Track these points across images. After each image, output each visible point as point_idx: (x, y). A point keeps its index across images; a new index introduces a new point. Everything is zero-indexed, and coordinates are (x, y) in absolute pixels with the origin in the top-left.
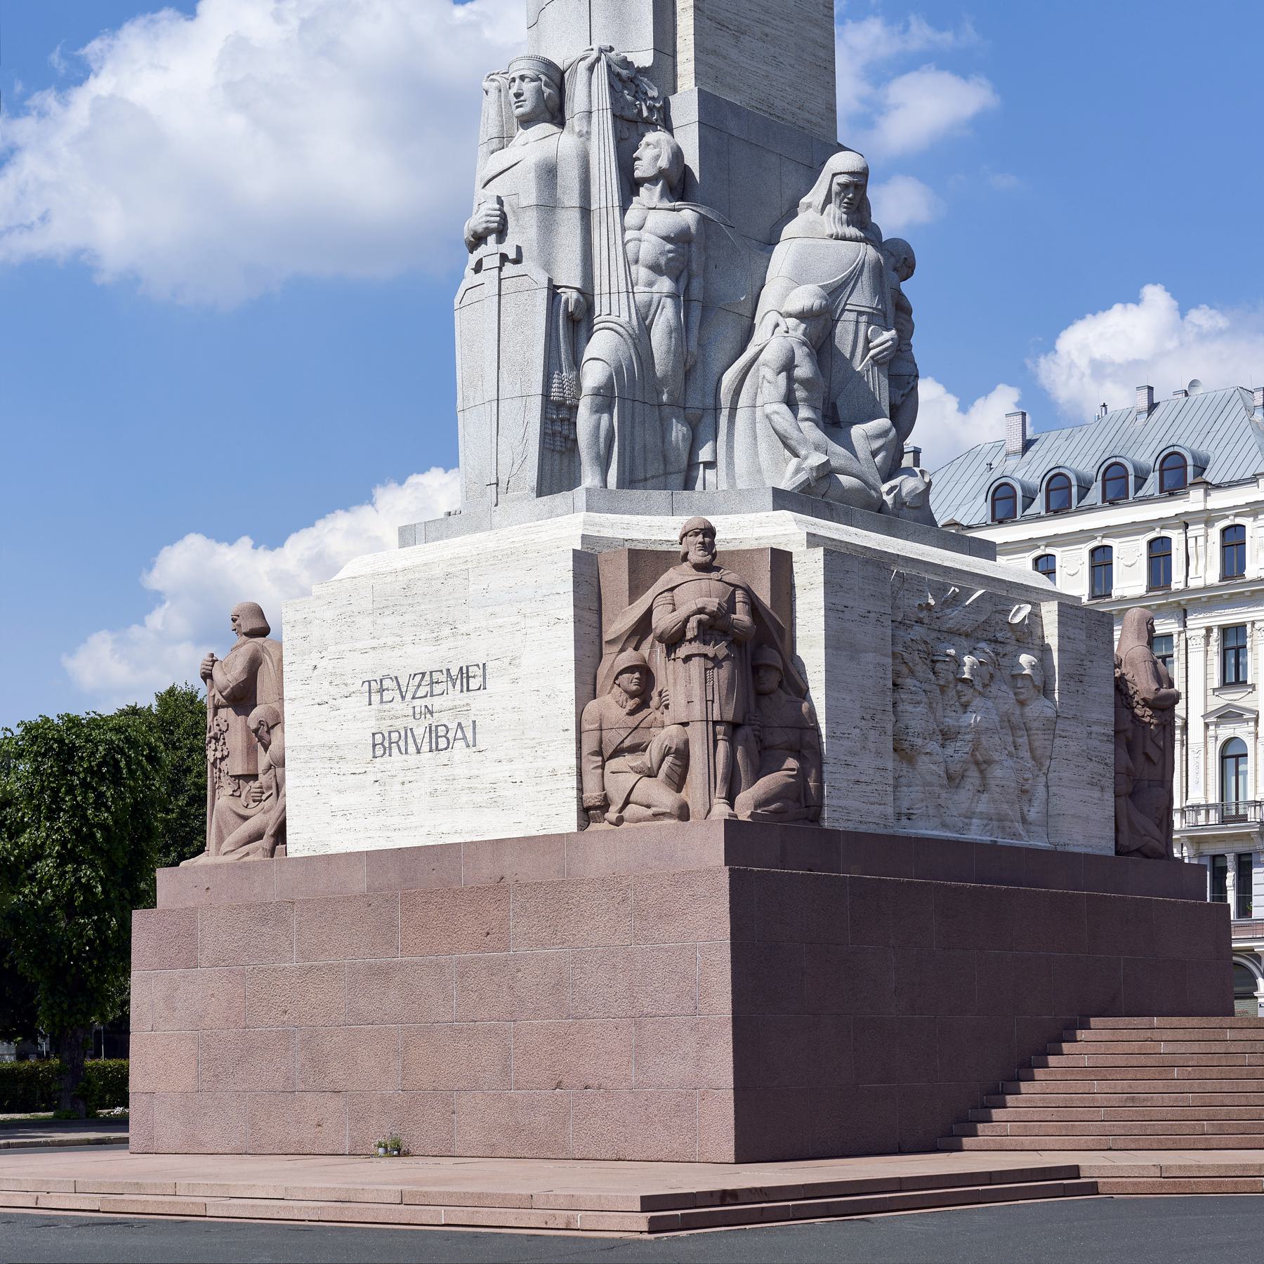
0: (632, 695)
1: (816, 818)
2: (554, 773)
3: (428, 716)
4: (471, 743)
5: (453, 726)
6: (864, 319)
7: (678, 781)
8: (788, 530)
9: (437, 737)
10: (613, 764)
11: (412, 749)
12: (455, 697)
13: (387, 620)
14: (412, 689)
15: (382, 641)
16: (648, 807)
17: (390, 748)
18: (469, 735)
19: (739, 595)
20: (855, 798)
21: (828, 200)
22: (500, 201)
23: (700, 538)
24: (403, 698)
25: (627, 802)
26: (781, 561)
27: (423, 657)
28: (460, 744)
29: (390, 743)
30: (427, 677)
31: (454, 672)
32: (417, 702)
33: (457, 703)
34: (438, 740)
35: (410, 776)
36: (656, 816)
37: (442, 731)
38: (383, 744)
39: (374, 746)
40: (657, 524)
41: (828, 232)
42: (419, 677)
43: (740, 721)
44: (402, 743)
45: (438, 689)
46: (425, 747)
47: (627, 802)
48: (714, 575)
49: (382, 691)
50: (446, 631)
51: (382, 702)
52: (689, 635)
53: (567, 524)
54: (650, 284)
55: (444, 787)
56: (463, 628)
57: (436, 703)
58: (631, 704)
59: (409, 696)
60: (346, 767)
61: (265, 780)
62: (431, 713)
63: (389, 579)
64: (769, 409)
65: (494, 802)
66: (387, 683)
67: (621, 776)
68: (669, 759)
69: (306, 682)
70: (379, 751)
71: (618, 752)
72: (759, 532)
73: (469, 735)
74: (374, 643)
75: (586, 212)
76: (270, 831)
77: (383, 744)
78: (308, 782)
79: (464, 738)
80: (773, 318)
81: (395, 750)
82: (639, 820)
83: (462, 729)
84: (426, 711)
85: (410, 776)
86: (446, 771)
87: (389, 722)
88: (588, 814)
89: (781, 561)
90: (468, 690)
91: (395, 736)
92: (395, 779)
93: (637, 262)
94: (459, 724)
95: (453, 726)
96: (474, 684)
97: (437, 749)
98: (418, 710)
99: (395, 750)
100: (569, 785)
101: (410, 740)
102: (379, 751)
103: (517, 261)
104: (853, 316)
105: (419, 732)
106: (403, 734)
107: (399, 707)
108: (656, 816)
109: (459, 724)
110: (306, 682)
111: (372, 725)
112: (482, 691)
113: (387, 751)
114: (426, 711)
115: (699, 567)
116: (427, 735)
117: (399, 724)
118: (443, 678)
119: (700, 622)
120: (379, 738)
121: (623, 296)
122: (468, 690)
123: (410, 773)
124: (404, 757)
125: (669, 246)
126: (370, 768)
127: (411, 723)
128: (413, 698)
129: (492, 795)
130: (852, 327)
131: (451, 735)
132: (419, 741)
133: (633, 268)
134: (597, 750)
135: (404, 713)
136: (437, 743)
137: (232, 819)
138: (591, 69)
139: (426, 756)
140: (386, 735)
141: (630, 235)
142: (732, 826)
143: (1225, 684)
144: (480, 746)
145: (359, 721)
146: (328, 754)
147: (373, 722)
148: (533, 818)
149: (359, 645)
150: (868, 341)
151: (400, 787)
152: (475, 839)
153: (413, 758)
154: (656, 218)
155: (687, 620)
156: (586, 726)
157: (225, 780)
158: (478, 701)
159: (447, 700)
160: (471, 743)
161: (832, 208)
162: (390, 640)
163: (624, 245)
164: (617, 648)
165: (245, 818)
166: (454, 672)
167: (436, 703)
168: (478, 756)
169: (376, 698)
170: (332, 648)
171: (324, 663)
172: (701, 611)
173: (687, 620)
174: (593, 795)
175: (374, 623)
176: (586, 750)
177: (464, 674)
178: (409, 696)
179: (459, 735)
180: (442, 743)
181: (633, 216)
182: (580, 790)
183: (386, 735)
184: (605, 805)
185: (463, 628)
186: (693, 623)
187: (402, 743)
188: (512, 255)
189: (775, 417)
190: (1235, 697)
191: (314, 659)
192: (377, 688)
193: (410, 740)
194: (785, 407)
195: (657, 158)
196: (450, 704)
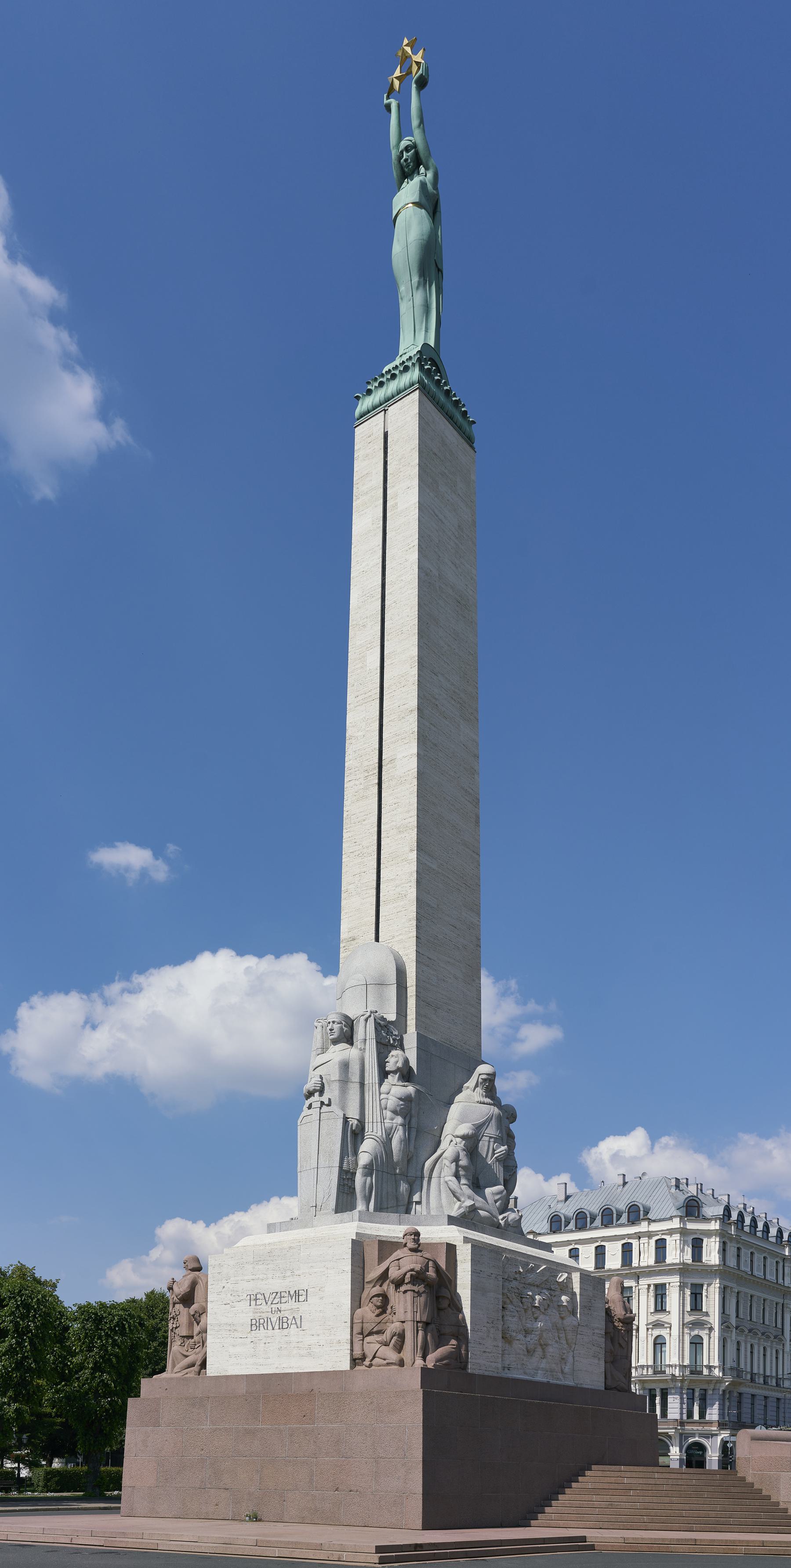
0: (378, 1307)
1: (465, 1368)
5: (290, 1317)
6: (492, 1140)
7: (399, 1348)
8: (454, 1234)
10: (368, 1339)
11: (270, 1327)
12: (292, 1304)
14: (271, 1299)
18: (299, 1323)
19: (431, 1264)
20: (483, 1360)
21: (476, 1086)
22: (321, 1077)
23: (413, 1237)
25: (374, 1357)
26: (451, 1249)
27: (277, 1284)
28: (294, 1326)
31: (292, 1293)
32: (273, 1306)
34: (283, 1324)
35: (269, 1340)
36: (388, 1364)
37: (285, 1320)
38: (256, 1325)
40: (393, 1229)
41: (476, 1100)
43: (429, 1321)
44: (265, 1325)
45: (283, 1300)
46: (277, 1327)
47: (374, 1357)
48: (419, 1254)
49: (256, 1299)
50: (289, 1273)
52: (406, 1281)
53: (349, 1227)
54: (392, 1119)
57: (283, 1307)
58: (378, 1311)
59: (269, 1303)
61: (197, 1338)
63: (262, 1248)
64: (447, 1179)
66: (259, 1296)
67: (372, 1345)
68: (395, 1338)
69: (219, 1294)
70: (254, 1328)
71: (370, 1334)
72: (441, 1235)
73: (299, 1323)
74: (253, 1277)
75: (362, 1084)
76: (198, 1363)
77: (256, 1325)
78: (218, 1341)
80: (450, 1137)
84: (276, 1311)
85: (269, 1340)
86: (286, 1339)
88: (355, 1361)
89: (451, 1249)
91: (262, 1321)
93: (386, 1109)
95: (290, 1317)
96: (301, 1298)
102: (254, 1328)
103: (329, 1105)
104: (487, 1139)
105: (274, 1320)
107: (264, 1307)
108: (388, 1364)
111: (251, 1315)
114: (276, 1311)
115: (411, 1250)
117: (264, 1315)
118: (286, 1295)
119: (411, 1275)
120: (254, 1322)
121: (379, 1124)
125: (401, 1103)
126: (249, 1335)
130: (487, 1144)
131: (289, 1322)
133: (384, 1111)
134: (360, 1332)
137: (180, 1356)
138: (366, 1020)
139: (277, 1331)
141: (383, 1096)
142: (425, 1370)
145: (244, 1313)
149: (246, 1278)
150: (494, 1150)
153: (270, 1332)
154: (396, 1090)
155: (405, 1274)
156: (355, 1321)
157: (177, 1338)
158: (303, 1307)
159: (288, 1306)
161: (478, 1089)
162: (261, 1277)
163: (380, 1101)
164: (371, 1285)
165: (186, 1356)
166: (292, 1293)
167: (283, 1307)
169: (253, 1303)
172: (412, 1270)
173: (405, 1274)
174: (358, 1353)
175: (254, 1268)
176: (355, 1332)
177: (297, 1294)
178: (269, 1303)
179: (294, 1322)
180: (285, 1325)
181: (384, 1088)
182: (352, 1350)
184: (364, 1358)
185: (297, 1273)
186: (408, 1275)
187: (265, 1325)
188: (326, 1102)
189: (450, 1183)
192: (254, 1298)
194: (454, 1179)
195: (397, 1062)
196: (290, 1308)
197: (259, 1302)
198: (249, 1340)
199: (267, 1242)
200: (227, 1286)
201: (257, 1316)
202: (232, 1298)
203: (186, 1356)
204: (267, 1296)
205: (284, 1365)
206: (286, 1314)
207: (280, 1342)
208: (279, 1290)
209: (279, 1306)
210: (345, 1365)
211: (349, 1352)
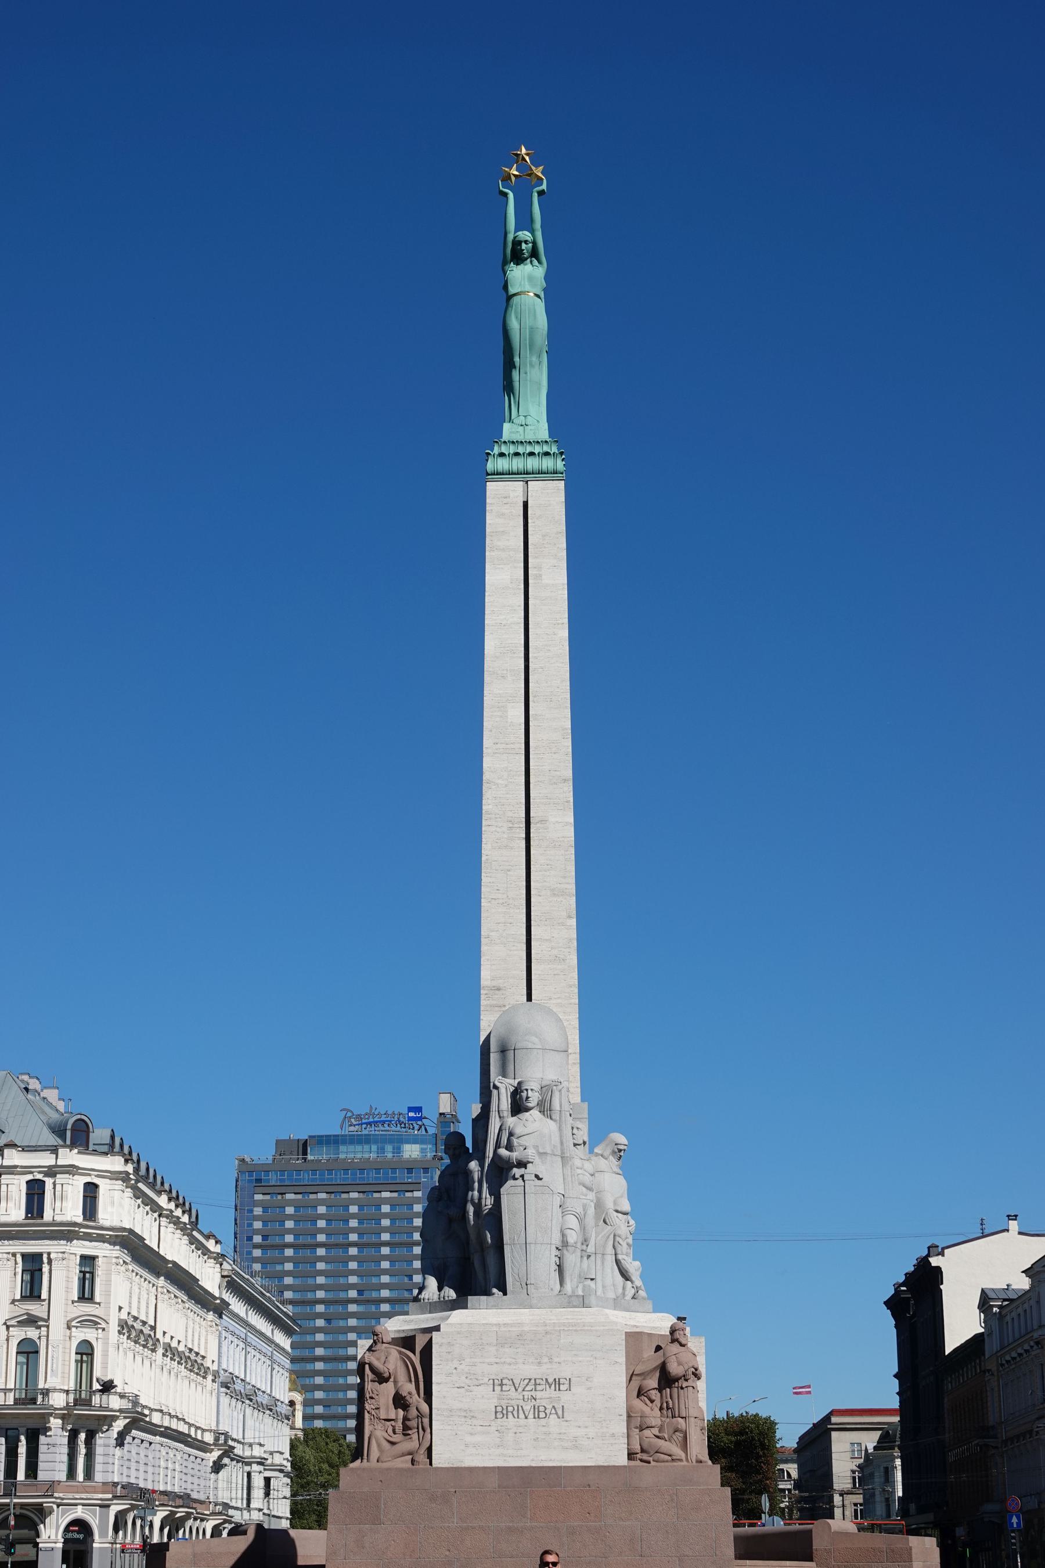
2: (613, 1435)
10: (647, 1433)
11: (522, 1415)
12: (551, 1392)
13: (507, 1350)
15: (503, 1360)
18: (560, 1413)
27: (530, 1370)
30: (533, 1381)
32: (525, 1393)
35: (520, 1430)
37: (542, 1409)
38: (502, 1412)
39: (496, 1412)
42: (526, 1381)
45: (539, 1388)
46: (531, 1416)
49: (501, 1385)
50: (546, 1360)
56: (556, 1360)
57: (538, 1395)
59: (520, 1389)
60: (475, 1422)
63: (495, 1329)
66: (504, 1382)
69: (450, 1374)
70: (499, 1415)
72: (657, 1324)
73: (560, 1413)
74: (497, 1360)
76: (423, 1450)
77: (502, 1412)
78: (450, 1427)
79: (556, 1413)
84: (528, 1398)
85: (520, 1430)
86: (544, 1429)
88: (631, 1456)
101: (521, 1411)
102: (499, 1415)
105: (527, 1408)
110: (450, 1374)
111: (495, 1402)
117: (513, 1403)
120: (499, 1409)
127: (521, 1403)
131: (548, 1411)
139: (531, 1420)
143: (24, 1298)
146: (464, 1414)
147: (495, 1400)
153: (522, 1421)
158: (565, 1397)
162: (508, 1360)
166: (551, 1380)
167: (538, 1395)
170: (468, 1360)
171: (462, 1367)
175: (497, 1350)
176: (632, 1425)
178: (520, 1389)
180: (542, 1415)
185: (556, 1360)
190: (35, 1309)
191: (456, 1364)
193: (521, 1411)
197: (504, 1388)
199: (494, 1320)
200: (460, 1368)
201: (504, 1403)
202: (468, 1381)
203: (393, 1443)
204: (517, 1382)
205: (543, 1458)
207: (535, 1432)
208: (533, 1377)
209: (533, 1393)
210: (622, 1460)
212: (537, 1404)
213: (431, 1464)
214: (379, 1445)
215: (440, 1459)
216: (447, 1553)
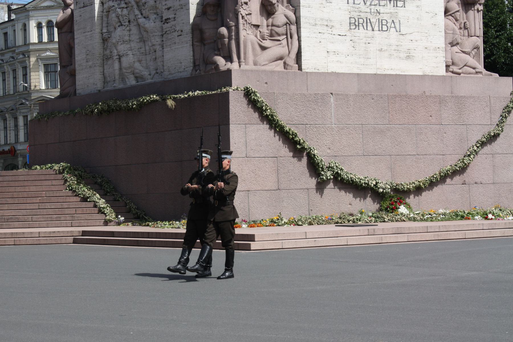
3: (378, 14)
4: (398, 30)
5: (390, 21)
9: (382, 25)
11: (370, 28)
16: (474, 68)
17: (359, 26)
24: (365, 4)
28: (393, 30)
29: (359, 23)
32: (373, 7)
33: (392, 11)
35: (369, 40)
37: (384, 22)
38: (355, 24)
39: (350, 23)
46: (376, 28)
51: (354, 3)
55: (385, 48)
57: (382, 9)
62: (379, 13)
65: (408, 57)
76: (293, 55)
77: (355, 24)
79: (395, 27)
81: (361, 27)
82: (470, 74)
83: (394, 23)
87: (359, 14)
90: (397, 6)
91: (361, 21)
92: (362, 41)
94: (393, 21)
97: (382, 30)
98: (372, 11)
99: (361, 27)
100: (442, 55)
101: (369, 24)
106: (365, 20)
108: (477, 73)
109: (393, 21)
112: (403, 8)
113: (357, 26)
116: (377, 23)
117: (363, 15)
120: (353, 21)
122: (397, 6)
123: (369, 39)
124: (366, 31)
126: (348, 34)
127: (369, 16)
128: (371, 5)
129: (408, 55)
131: (389, 25)
132: (373, 25)
135: (365, 11)
136: (382, 27)
139: (376, 33)
140: (357, 19)
144: (403, 32)
146: (326, 23)
148: (427, 67)
151: (364, 45)
152: (401, 73)
153: (370, 33)
160: (398, 30)
167: (382, 9)
168: (401, 37)
179: (393, 25)
180: (385, 28)
183: (357, 19)
187: (365, 25)
193: (369, 24)
198: (348, 38)
201: (355, 15)
206: (385, 17)
209: (378, 8)
210: (442, 71)
211: (444, 59)
212: (381, 17)
213: (300, 68)
214: (254, 49)
215: (308, 63)
216: (329, 151)
